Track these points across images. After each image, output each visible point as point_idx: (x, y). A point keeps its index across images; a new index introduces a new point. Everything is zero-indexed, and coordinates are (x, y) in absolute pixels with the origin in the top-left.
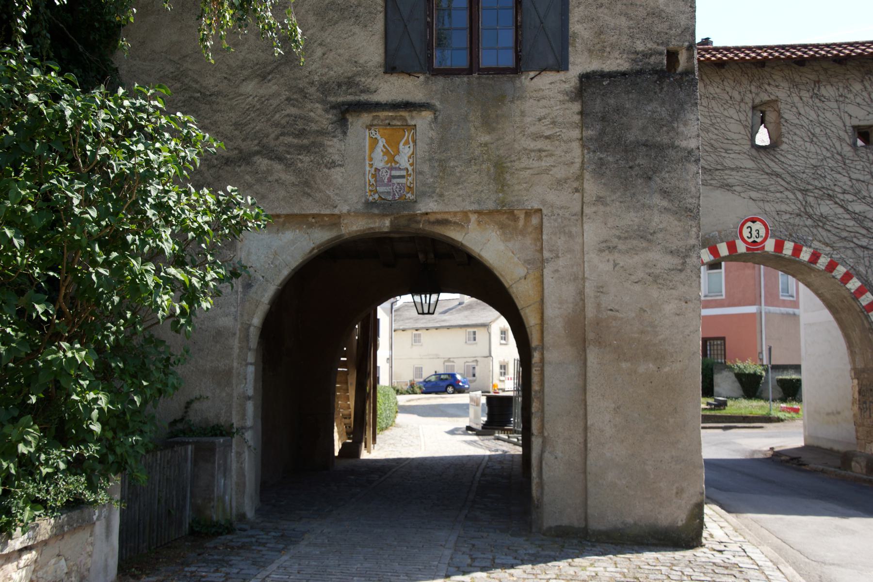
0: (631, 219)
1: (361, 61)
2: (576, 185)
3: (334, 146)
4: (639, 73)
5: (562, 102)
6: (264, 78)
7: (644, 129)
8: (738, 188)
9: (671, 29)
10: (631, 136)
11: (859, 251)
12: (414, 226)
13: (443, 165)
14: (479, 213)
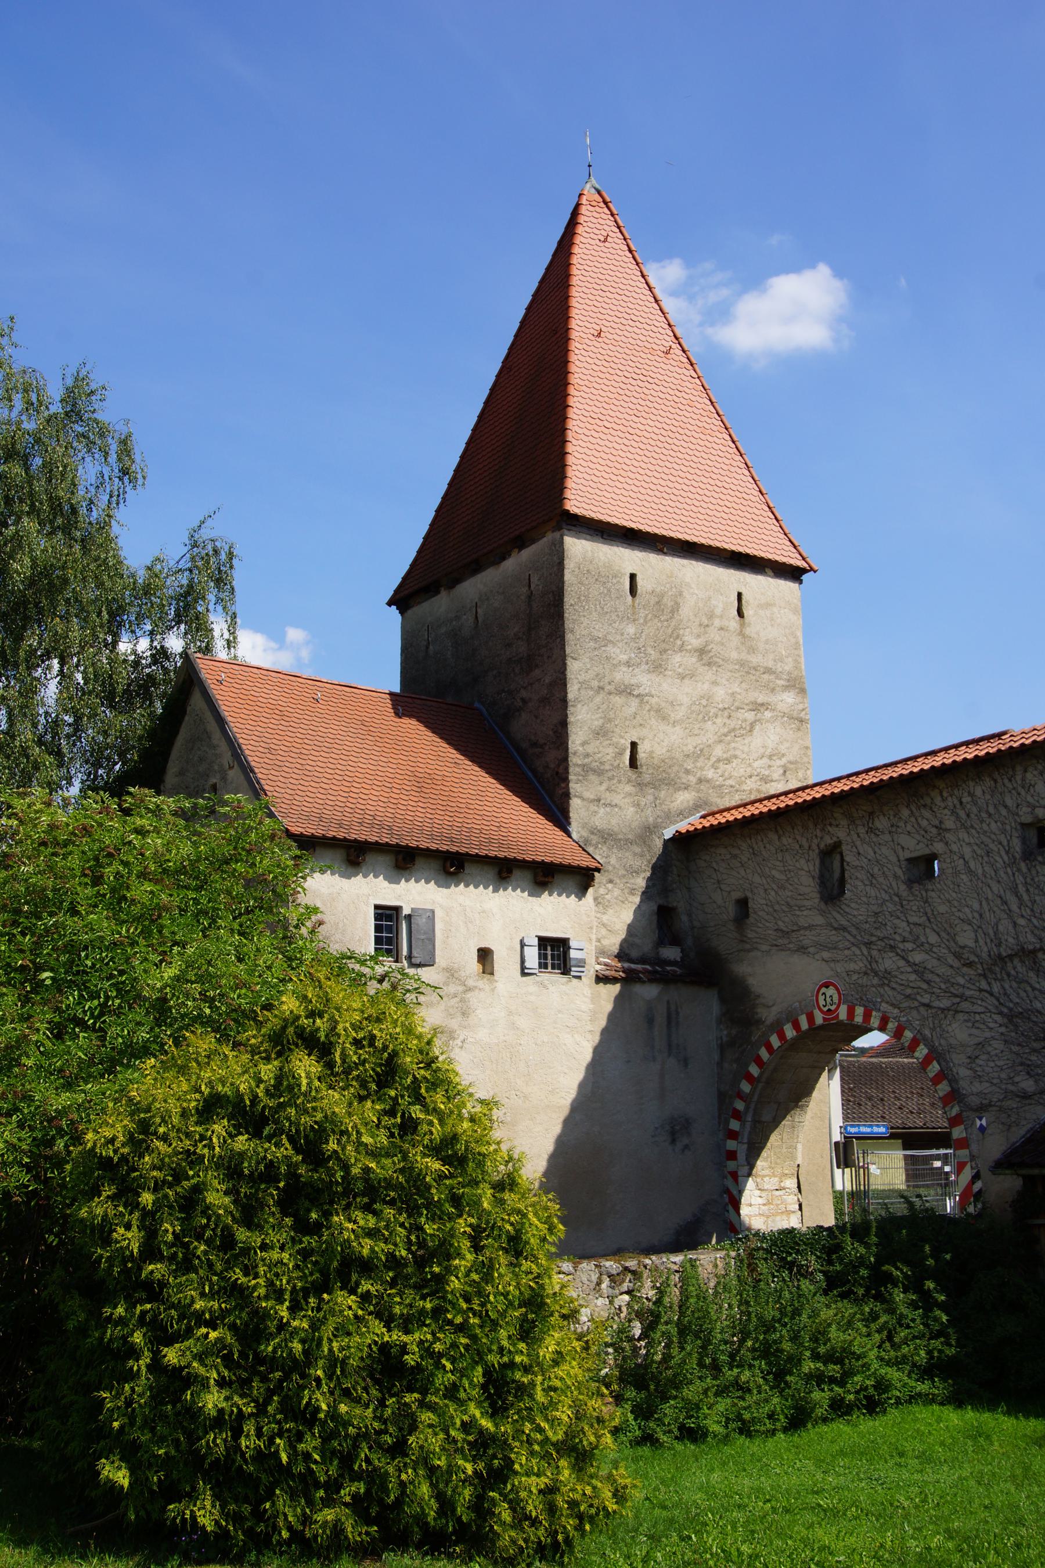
8: (811, 950)
11: (922, 1009)
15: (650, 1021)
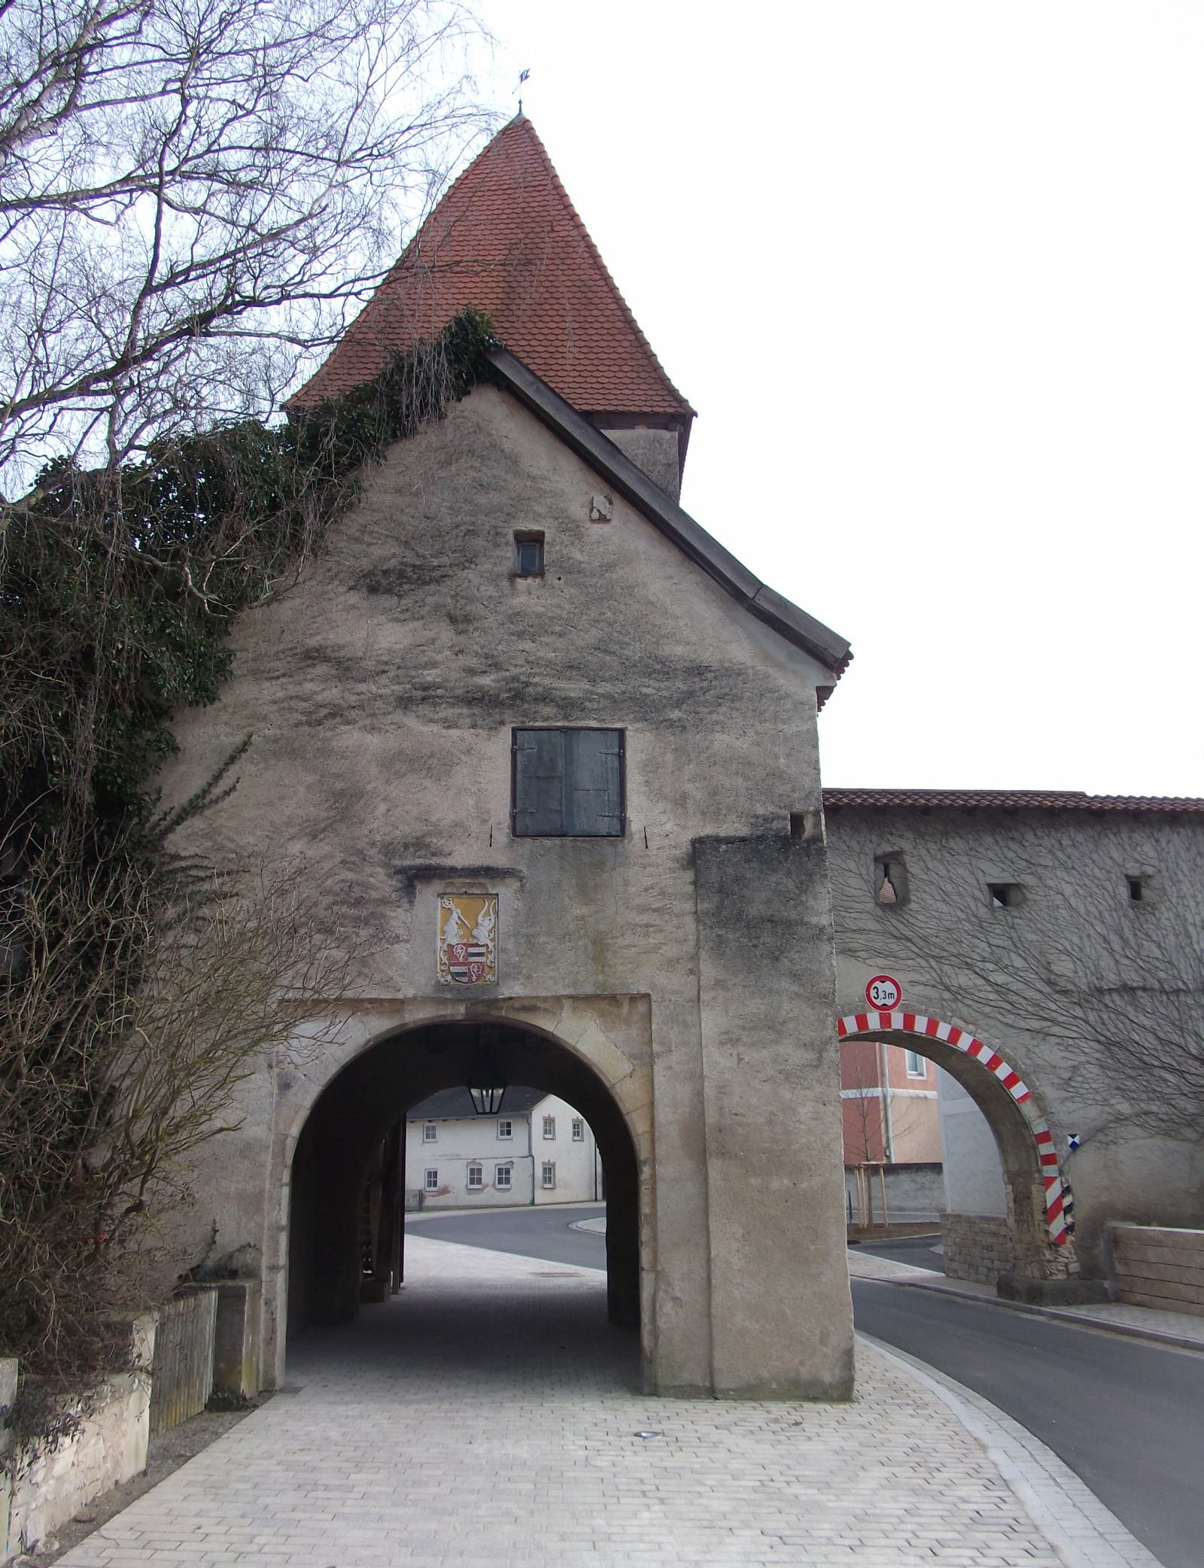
0: (756, 1006)
1: (433, 819)
2: (690, 966)
3: (398, 918)
4: (761, 839)
5: (672, 870)
6: (315, 837)
7: (769, 902)
9: (793, 791)
10: (754, 910)
12: (495, 1013)
13: (530, 941)
14: (574, 998)
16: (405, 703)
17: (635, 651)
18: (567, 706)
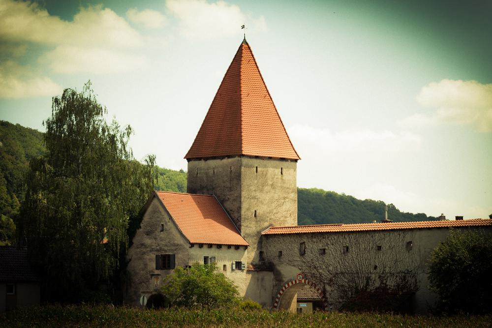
15: (258, 280)
16: (151, 251)
17: (172, 242)
18: (166, 251)
